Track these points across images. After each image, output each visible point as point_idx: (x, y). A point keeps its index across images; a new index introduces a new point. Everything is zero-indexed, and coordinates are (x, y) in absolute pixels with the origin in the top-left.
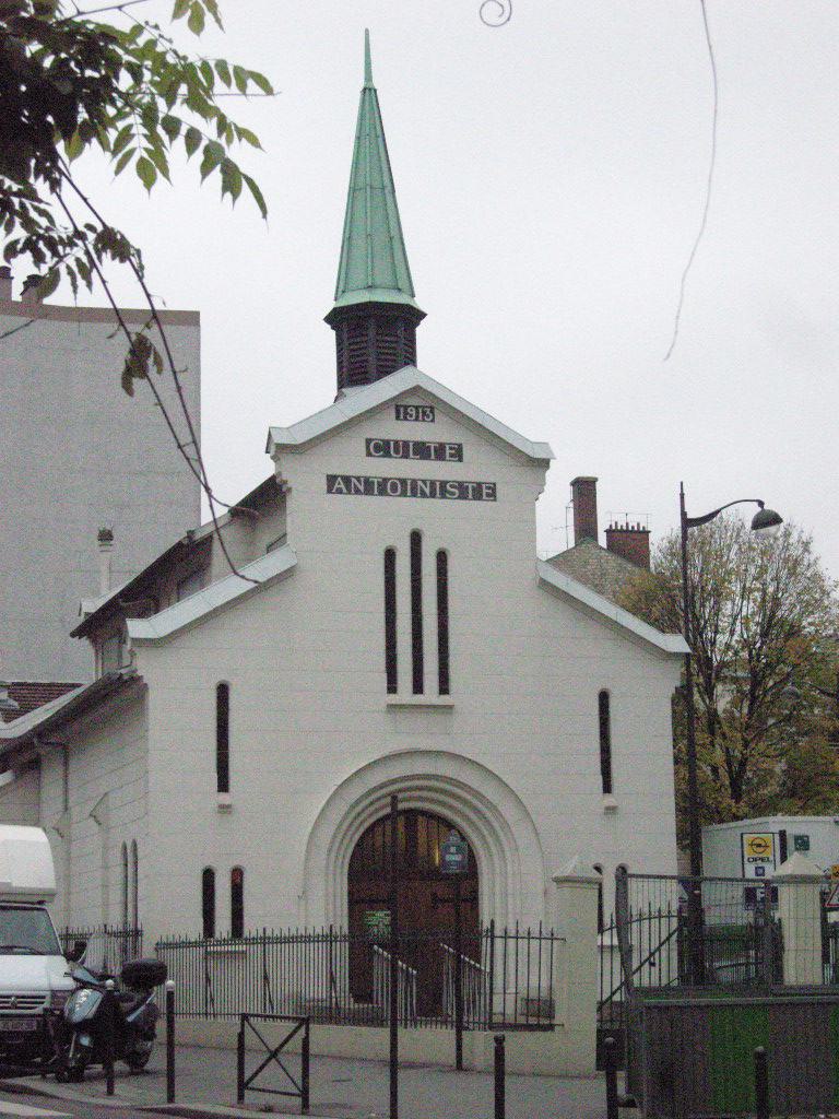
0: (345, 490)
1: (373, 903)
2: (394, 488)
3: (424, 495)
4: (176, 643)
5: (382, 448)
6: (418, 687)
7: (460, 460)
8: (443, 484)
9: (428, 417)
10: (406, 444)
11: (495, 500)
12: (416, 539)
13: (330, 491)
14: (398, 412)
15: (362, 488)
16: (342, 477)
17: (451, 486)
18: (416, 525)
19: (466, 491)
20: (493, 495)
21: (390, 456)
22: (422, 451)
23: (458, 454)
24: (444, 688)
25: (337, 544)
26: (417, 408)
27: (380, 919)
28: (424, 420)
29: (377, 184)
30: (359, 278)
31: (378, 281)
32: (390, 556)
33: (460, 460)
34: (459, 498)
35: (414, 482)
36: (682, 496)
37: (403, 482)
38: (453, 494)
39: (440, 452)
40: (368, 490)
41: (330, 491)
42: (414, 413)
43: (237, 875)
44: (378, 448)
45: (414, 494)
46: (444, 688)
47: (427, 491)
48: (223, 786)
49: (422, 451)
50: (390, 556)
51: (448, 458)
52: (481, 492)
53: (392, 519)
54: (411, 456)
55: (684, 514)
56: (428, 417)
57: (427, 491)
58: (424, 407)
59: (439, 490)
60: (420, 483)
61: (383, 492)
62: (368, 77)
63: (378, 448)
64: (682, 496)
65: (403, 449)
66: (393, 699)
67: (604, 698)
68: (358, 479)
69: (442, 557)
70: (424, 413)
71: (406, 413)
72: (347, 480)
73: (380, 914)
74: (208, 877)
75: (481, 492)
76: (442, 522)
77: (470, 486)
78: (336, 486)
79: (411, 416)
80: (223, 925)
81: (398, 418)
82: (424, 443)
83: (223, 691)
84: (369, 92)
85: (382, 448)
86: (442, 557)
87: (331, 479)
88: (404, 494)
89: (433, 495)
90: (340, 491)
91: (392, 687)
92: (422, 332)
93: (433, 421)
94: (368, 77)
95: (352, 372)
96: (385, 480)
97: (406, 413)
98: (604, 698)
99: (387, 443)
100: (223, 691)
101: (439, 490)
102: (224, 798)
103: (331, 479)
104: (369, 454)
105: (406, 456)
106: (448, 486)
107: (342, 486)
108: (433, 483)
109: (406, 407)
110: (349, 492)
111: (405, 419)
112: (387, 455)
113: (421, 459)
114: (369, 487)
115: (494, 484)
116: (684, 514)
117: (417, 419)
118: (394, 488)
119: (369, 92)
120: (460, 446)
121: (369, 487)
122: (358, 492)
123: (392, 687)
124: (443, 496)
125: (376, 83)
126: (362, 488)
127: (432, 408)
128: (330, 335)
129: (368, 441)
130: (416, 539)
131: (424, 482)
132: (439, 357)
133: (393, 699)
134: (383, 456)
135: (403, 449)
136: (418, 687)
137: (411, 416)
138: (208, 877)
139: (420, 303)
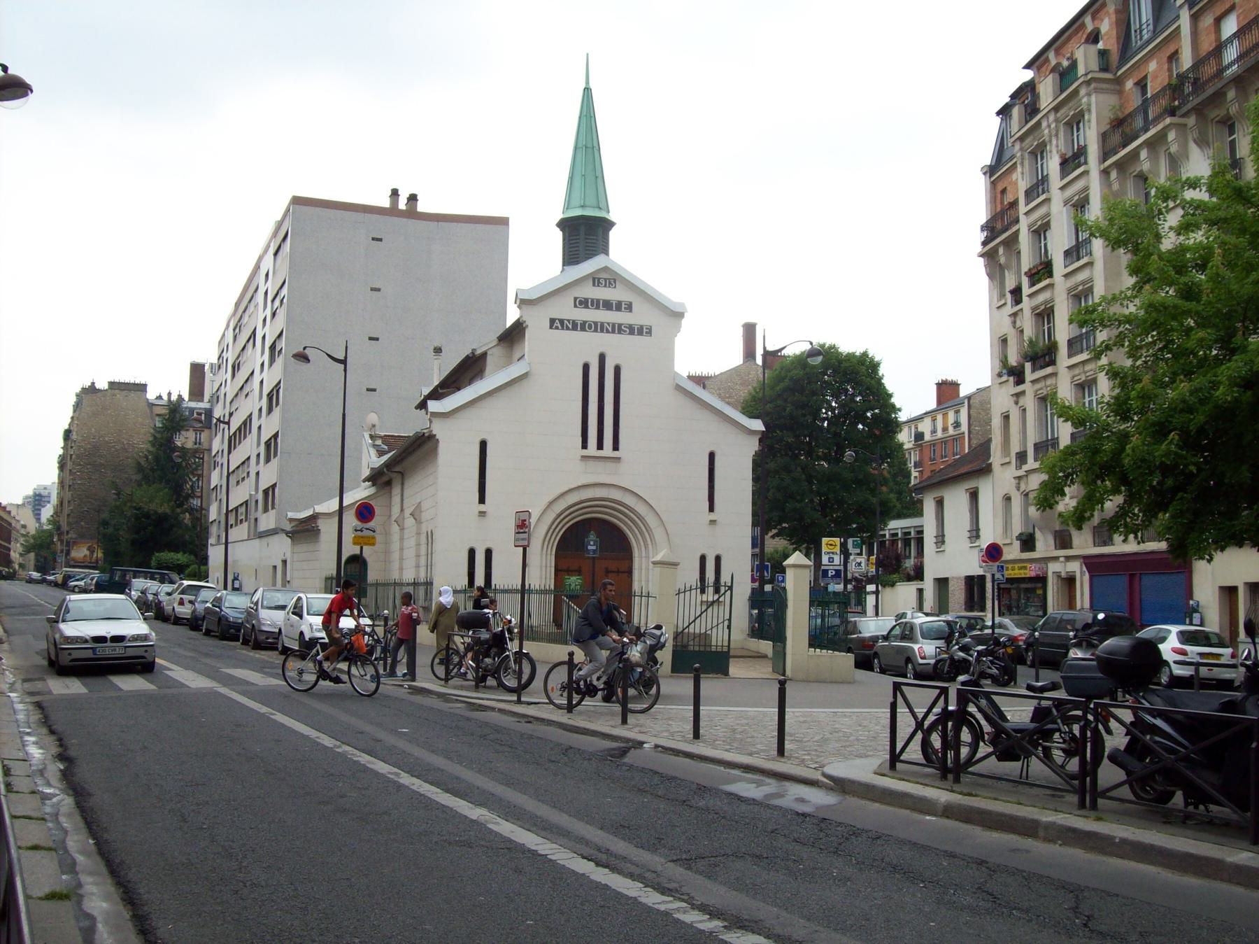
1: (570, 572)
2: (590, 327)
3: (608, 331)
4: (457, 415)
5: (584, 303)
6: (600, 446)
8: (620, 325)
10: (598, 301)
12: (602, 358)
19: (631, 330)
20: (649, 333)
22: (608, 305)
23: (629, 307)
24: (616, 447)
25: (555, 361)
27: (574, 581)
29: (589, 145)
30: (576, 200)
31: (587, 203)
32: (586, 368)
35: (602, 324)
37: (596, 323)
39: (619, 306)
40: (575, 327)
43: (489, 553)
44: (581, 303)
45: (602, 331)
46: (616, 447)
48: (482, 500)
49: (608, 305)
50: (586, 368)
52: (641, 331)
53: (587, 346)
59: (617, 329)
61: (583, 329)
62: (587, 82)
63: (581, 303)
65: (596, 304)
66: (585, 452)
67: (712, 456)
69: (617, 370)
72: (562, 321)
73: (574, 578)
74: (472, 553)
75: (641, 331)
76: (618, 349)
80: (480, 581)
83: (483, 445)
84: (587, 91)
85: (584, 303)
86: (617, 370)
88: (596, 331)
89: (613, 332)
90: (557, 328)
91: (585, 445)
92: (613, 234)
94: (587, 82)
95: (572, 256)
96: (585, 322)
98: (712, 456)
99: (586, 300)
100: (483, 445)
101: (617, 329)
102: (482, 508)
103: (552, 321)
105: (598, 308)
108: (614, 325)
112: (587, 307)
114: (574, 326)
118: (590, 327)
119: (587, 91)
121: (574, 326)
122: (568, 328)
123: (585, 445)
125: (592, 85)
128: (558, 235)
129: (575, 299)
130: (602, 358)
132: (623, 251)
133: (585, 452)
135: (596, 304)
136: (600, 446)
138: (472, 553)
139: (612, 216)
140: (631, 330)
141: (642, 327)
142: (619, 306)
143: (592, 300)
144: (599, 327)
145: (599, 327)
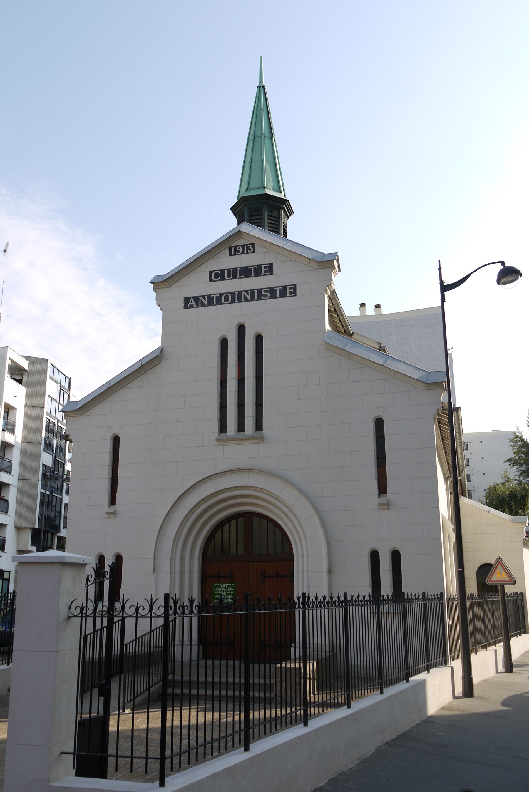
0: (195, 305)
2: (227, 299)
3: (246, 300)
5: (219, 275)
7: (272, 273)
8: (259, 291)
9: (250, 250)
10: (235, 270)
11: (295, 295)
12: (241, 329)
13: (185, 307)
14: (230, 249)
15: (206, 302)
16: (193, 297)
17: (264, 291)
18: (241, 320)
19: (273, 293)
20: (294, 291)
21: (225, 279)
22: (246, 272)
23: (270, 269)
26: (243, 246)
28: (247, 253)
32: (224, 342)
33: (272, 273)
34: (269, 298)
35: (240, 293)
36: (440, 269)
37: (233, 294)
38: (267, 296)
39: (258, 271)
41: (185, 307)
42: (241, 250)
44: (216, 275)
45: (240, 301)
47: (249, 297)
49: (246, 272)
50: (224, 342)
51: (263, 274)
52: (286, 291)
54: (238, 277)
55: (442, 282)
56: (250, 250)
57: (249, 297)
58: (247, 245)
60: (244, 293)
61: (219, 302)
63: (216, 275)
64: (440, 269)
65: (233, 274)
68: (203, 297)
69: (259, 339)
70: (248, 248)
71: (236, 250)
72: (196, 299)
75: (286, 291)
76: (257, 316)
77: (278, 289)
78: (190, 303)
79: (239, 252)
81: (230, 254)
82: (247, 267)
85: (219, 275)
86: (259, 339)
87: (187, 300)
88: (233, 301)
89: (252, 299)
90: (192, 306)
93: (253, 252)
96: (221, 295)
97: (236, 250)
98: (379, 424)
99: (223, 271)
100: (116, 440)
101: (257, 295)
103: (187, 300)
104: (211, 280)
105: (235, 277)
106: (263, 292)
107: (194, 303)
108: (252, 292)
109: (236, 247)
110: (198, 306)
111: (235, 254)
112: (223, 279)
113: (245, 277)
114: (210, 301)
115: (295, 285)
116: (442, 282)
117: (243, 253)
118: (227, 299)
120: (271, 265)
121: (210, 301)
122: (203, 305)
124: (259, 299)
126: (206, 302)
127: (253, 245)
129: (211, 273)
130: (241, 329)
131: (247, 292)
134: (220, 280)
135: (233, 274)
137: (239, 252)
140: (273, 293)
141: (284, 287)
142: (258, 271)
143: (229, 270)
144: (237, 297)
145: (237, 297)
